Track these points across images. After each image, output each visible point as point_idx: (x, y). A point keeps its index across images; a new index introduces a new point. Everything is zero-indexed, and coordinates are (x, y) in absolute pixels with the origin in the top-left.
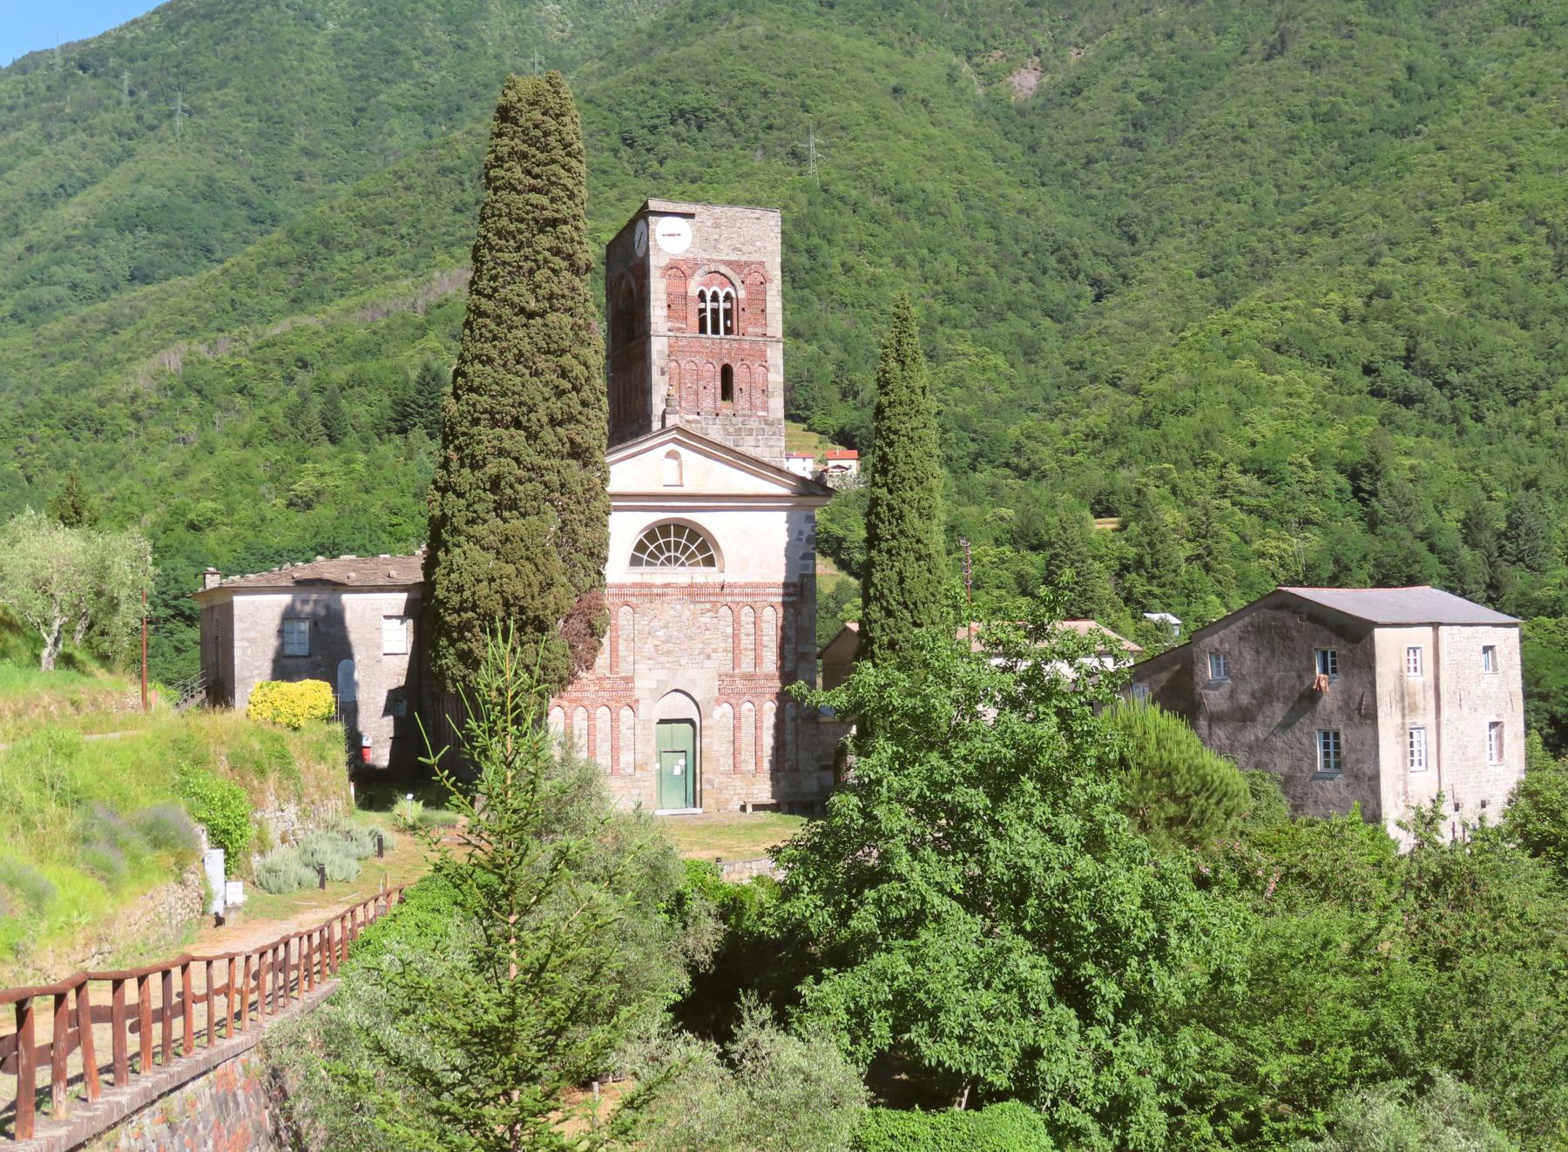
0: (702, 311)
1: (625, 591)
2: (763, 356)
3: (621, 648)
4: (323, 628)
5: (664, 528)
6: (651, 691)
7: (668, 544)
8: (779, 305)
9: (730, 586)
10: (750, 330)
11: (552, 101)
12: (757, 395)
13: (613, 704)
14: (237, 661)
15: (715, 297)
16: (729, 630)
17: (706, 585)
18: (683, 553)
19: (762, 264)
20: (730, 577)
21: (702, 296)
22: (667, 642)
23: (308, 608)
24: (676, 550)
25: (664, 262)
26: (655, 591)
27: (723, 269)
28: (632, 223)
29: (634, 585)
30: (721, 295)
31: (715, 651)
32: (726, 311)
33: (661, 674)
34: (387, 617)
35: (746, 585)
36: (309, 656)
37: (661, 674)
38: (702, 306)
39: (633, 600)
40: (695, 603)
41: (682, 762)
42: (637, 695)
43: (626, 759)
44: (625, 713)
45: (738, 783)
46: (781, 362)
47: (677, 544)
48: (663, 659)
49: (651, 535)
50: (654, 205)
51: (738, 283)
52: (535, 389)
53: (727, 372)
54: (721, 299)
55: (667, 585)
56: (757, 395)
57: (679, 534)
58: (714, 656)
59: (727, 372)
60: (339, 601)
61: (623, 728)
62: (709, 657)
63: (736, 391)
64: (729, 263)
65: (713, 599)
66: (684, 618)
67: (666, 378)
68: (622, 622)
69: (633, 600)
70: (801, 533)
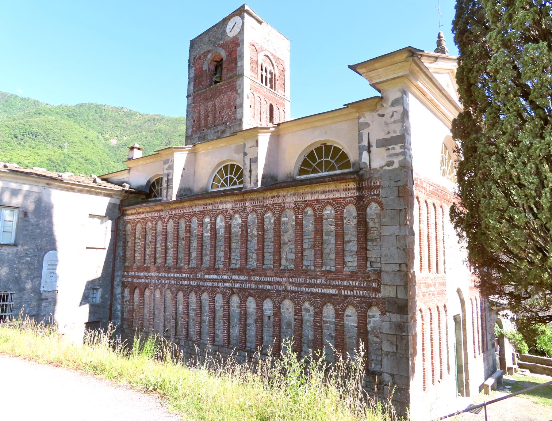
0: (262, 75)
4: (32, 219)
23: (17, 201)
34: (92, 216)
36: (15, 245)
60: (49, 195)
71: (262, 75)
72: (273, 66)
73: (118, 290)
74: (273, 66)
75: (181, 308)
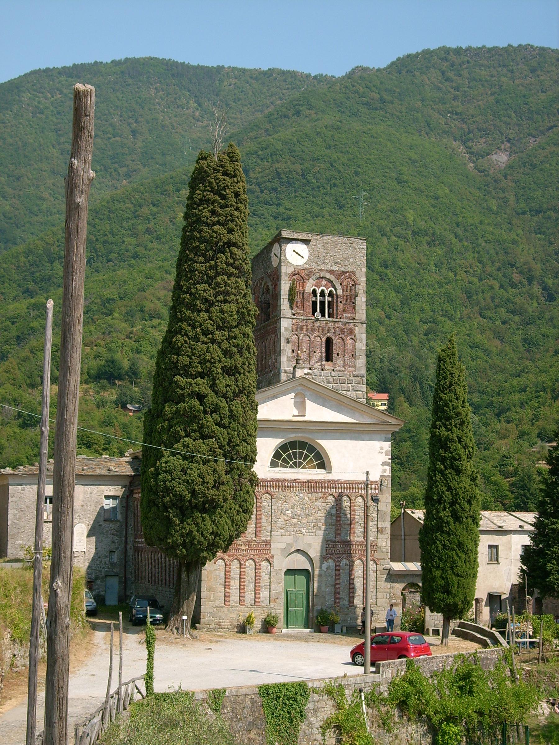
0: (314, 303)
1: (268, 484)
2: (352, 332)
3: (263, 520)
5: (293, 444)
6: (283, 550)
7: (295, 454)
8: (364, 299)
10: (345, 315)
11: (230, 168)
12: (348, 358)
14: (9, 523)
15: (322, 294)
18: (304, 460)
19: (354, 273)
20: (335, 475)
21: (314, 292)
24: (300, 458)
25: (290, 270)
26: (286, 484)
27: (328, 276)
28: (271, 244)
29: (273, 480)
30: (327, 292)
32: (329, 302)
33: (289, 539)
37: (289, 539)
38: (314, 299)
39: (271, 490)
43: (264, 594)
44: (265, 564)
46: (364, 336)
47: (301, 454)
48: (291, 529)
49: (284, 448)
50: (285, 234)
51: (338, 286)
52: (216, 352)
53: (329, 343)
54: (327, 295)
56: (348, 358)
59: (329, 343)
61: (263, 574)
63: (335, 356)
64: (332, 272)
65: (324, 490)
67: (290, 345)
68: (264, 503)
69: (271, 490)
70: (381, 448)
71: (314, 303)
72: (334, 286)
73: (130, 552)
74: (334, 286)
75: (153, 563)
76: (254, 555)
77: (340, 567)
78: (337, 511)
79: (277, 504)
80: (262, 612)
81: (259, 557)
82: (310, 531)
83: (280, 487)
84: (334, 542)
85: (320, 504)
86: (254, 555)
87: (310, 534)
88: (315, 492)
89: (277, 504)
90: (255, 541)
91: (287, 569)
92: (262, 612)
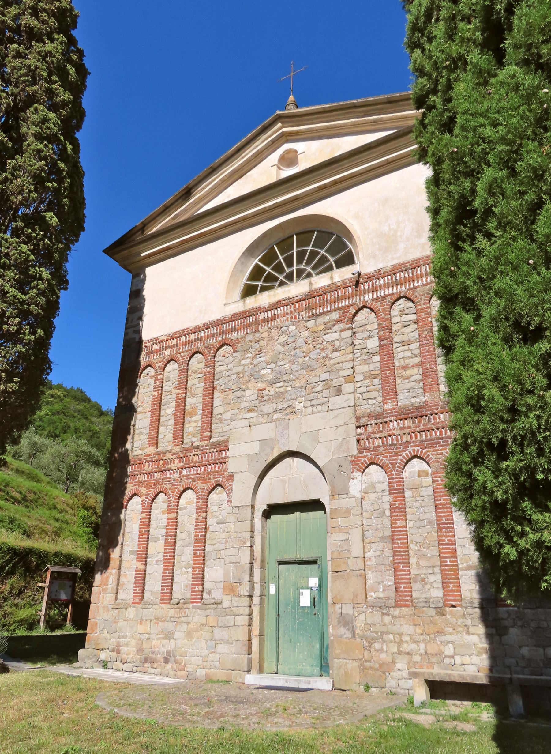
3: (216, 403)
6: (251, 458)
9: (370, 278)
13: (199, 485)
16: (373, 344)
17: (333, 288)
22: (276, 381)
26: (261, 316)
29: (235, 317)
31: (351, 379)
35: (395, 270)
39: (235, 335)
40: (315, 316)
41: (313, 582)
42: (231, 467)
45: (407, 629)
47: (301, 255)
48: (269, 408)
55: (278, 304)
57: (304, 240)
58: (348, 388)
62: (339, 391)
65: (343, 304)
66: (301, 342)
76: (194, 480)
77: (401, 480)
78: (380, 340)
79: (244, 362)
80: (204, 620)
81: (205, 481)
82: (314, 402)
83: (249, 325)
84: (379, 415)
85: (336, 336)
86: (194, 480)
87: (314, 408)
88: (323, 313)
89: (244, 362)
90: (197, 447)
91: (269, 506)
92: (204, 620)
